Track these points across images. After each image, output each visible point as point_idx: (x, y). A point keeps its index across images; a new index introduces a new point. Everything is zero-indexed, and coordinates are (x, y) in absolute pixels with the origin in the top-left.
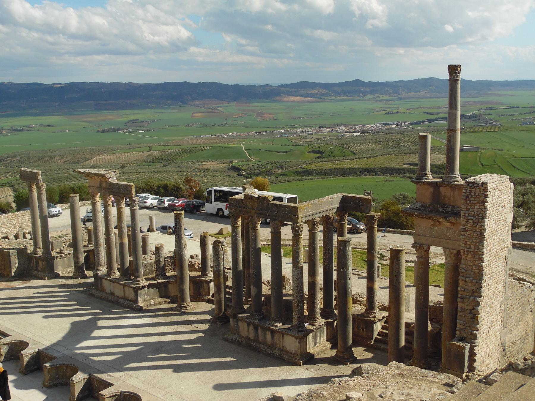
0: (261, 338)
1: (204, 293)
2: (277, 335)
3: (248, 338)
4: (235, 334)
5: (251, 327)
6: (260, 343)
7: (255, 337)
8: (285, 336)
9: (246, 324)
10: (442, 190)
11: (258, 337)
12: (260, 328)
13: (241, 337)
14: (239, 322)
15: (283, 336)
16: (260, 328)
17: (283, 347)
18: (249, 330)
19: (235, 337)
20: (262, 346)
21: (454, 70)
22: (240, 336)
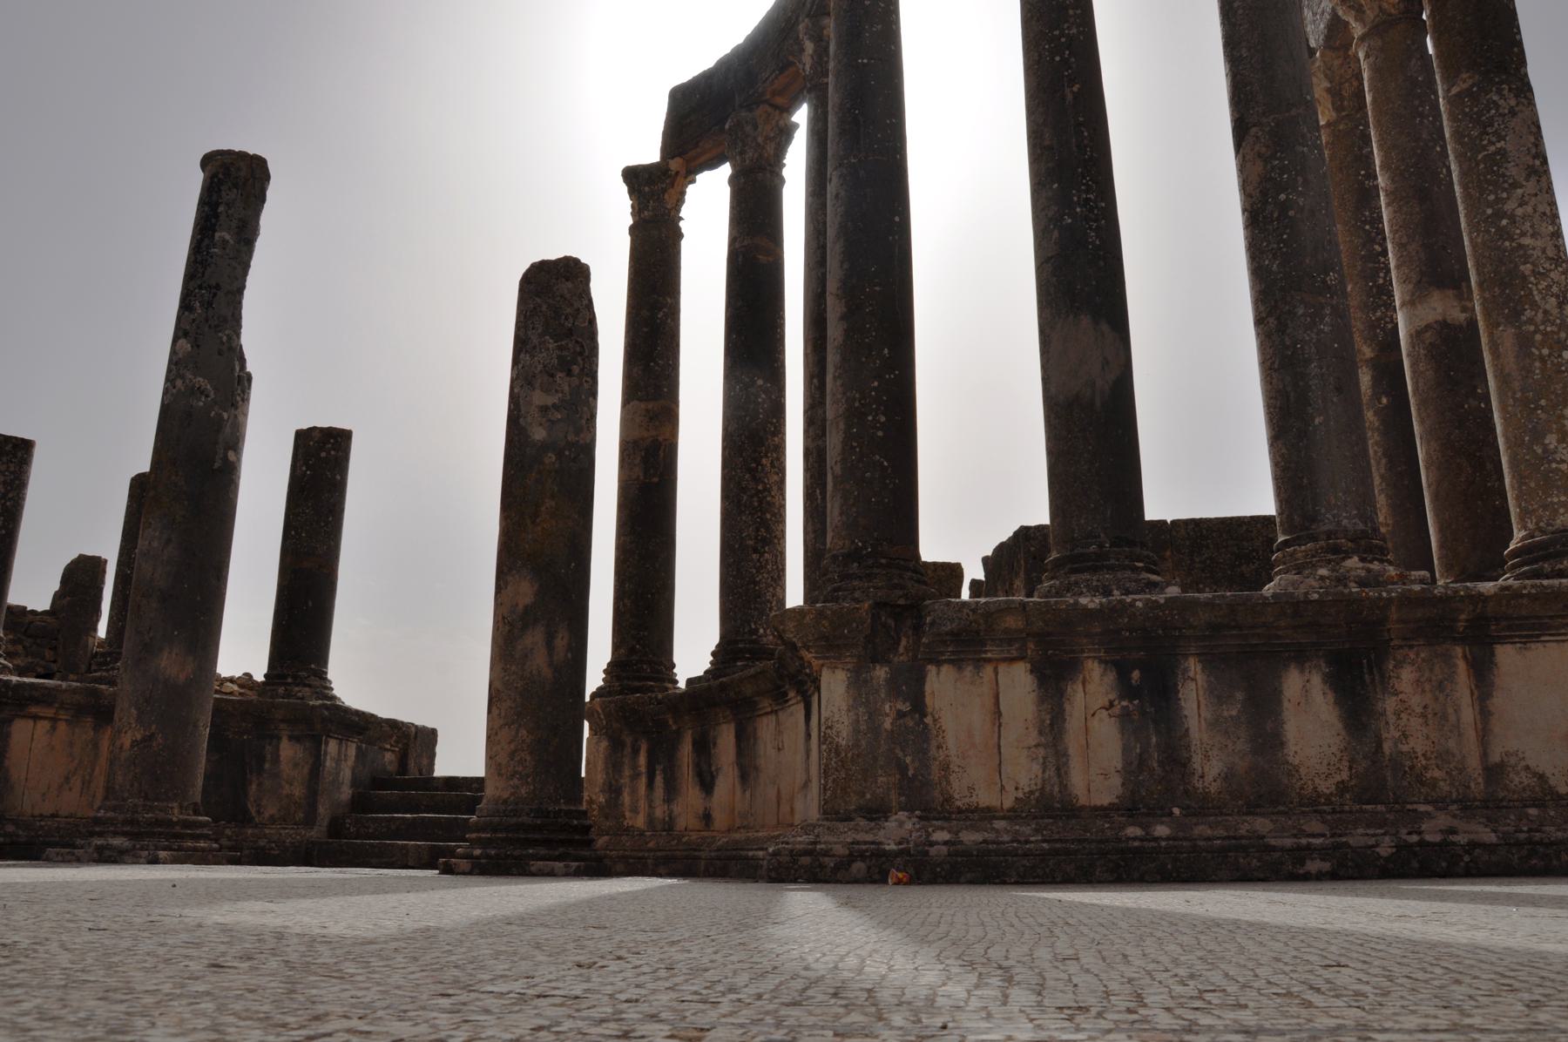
1: (271, 810)
2: (1407, 675)
4: (876, 812)
5: (1093, 691)
6: (1203, 807)
7: (1134, 768)
8: (1506, 655)
9: (1018, 683)
11: (1176, 758)
12: (1193, 666)
13: (982, 815)
14: (942, 685)
15: (1482, 671)
16: (1193, 666)
17: (1495, 772)
18: (1053, 726)
19: (897, 830)
20: (1262, 824)
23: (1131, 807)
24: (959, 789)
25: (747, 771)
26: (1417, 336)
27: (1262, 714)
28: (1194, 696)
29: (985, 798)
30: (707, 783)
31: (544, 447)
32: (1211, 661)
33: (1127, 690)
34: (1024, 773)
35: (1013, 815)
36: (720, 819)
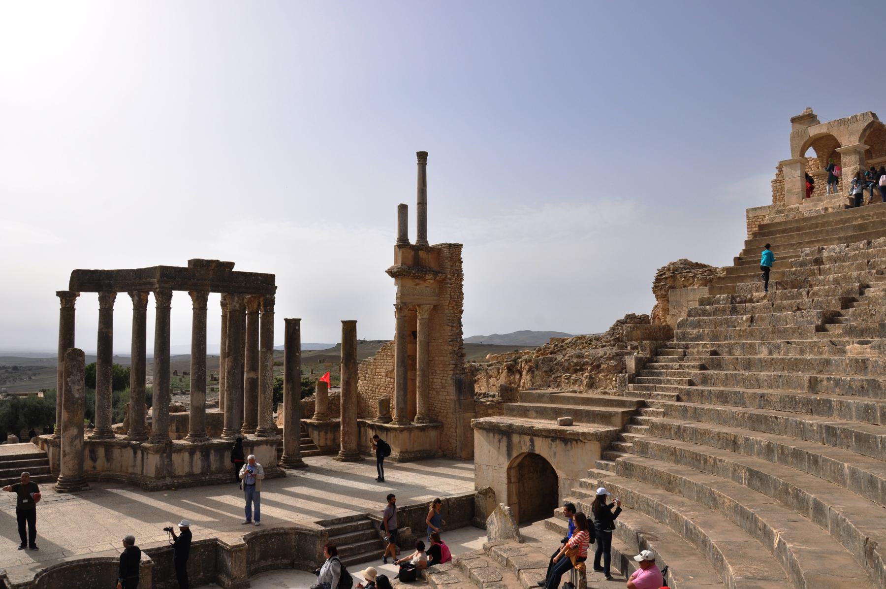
0: (214, 466)
3: (190, 475)
4: (164, 478)
5: (198, 456)
6: (212, 473)
7: (203, 468)
8: (255, 448)
9: (186, 455)
10: (420, 253)
11: (209, 466)
13: (181, 477)
14: (175, 456)
19: (168, 481)
20: (221, 475)
21: (422, 157)
22: (173, 477)
23: (203, 474)
24: (177, 473)
25: (109, 458)
26: (248, 379)
27: (222, 458)
28: (212, 456)
29: (181, 474)
30: (94, 459)
31: (78, 399)
32: (215, 451)
33: (203, 456)
34: (187, 469)
35: (185, 476)
36: (99, 468)
